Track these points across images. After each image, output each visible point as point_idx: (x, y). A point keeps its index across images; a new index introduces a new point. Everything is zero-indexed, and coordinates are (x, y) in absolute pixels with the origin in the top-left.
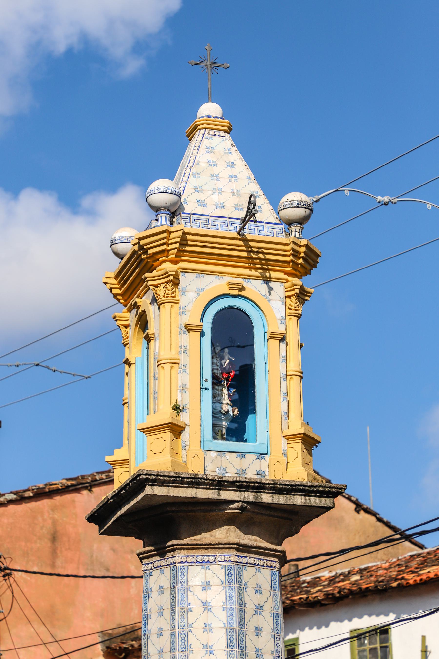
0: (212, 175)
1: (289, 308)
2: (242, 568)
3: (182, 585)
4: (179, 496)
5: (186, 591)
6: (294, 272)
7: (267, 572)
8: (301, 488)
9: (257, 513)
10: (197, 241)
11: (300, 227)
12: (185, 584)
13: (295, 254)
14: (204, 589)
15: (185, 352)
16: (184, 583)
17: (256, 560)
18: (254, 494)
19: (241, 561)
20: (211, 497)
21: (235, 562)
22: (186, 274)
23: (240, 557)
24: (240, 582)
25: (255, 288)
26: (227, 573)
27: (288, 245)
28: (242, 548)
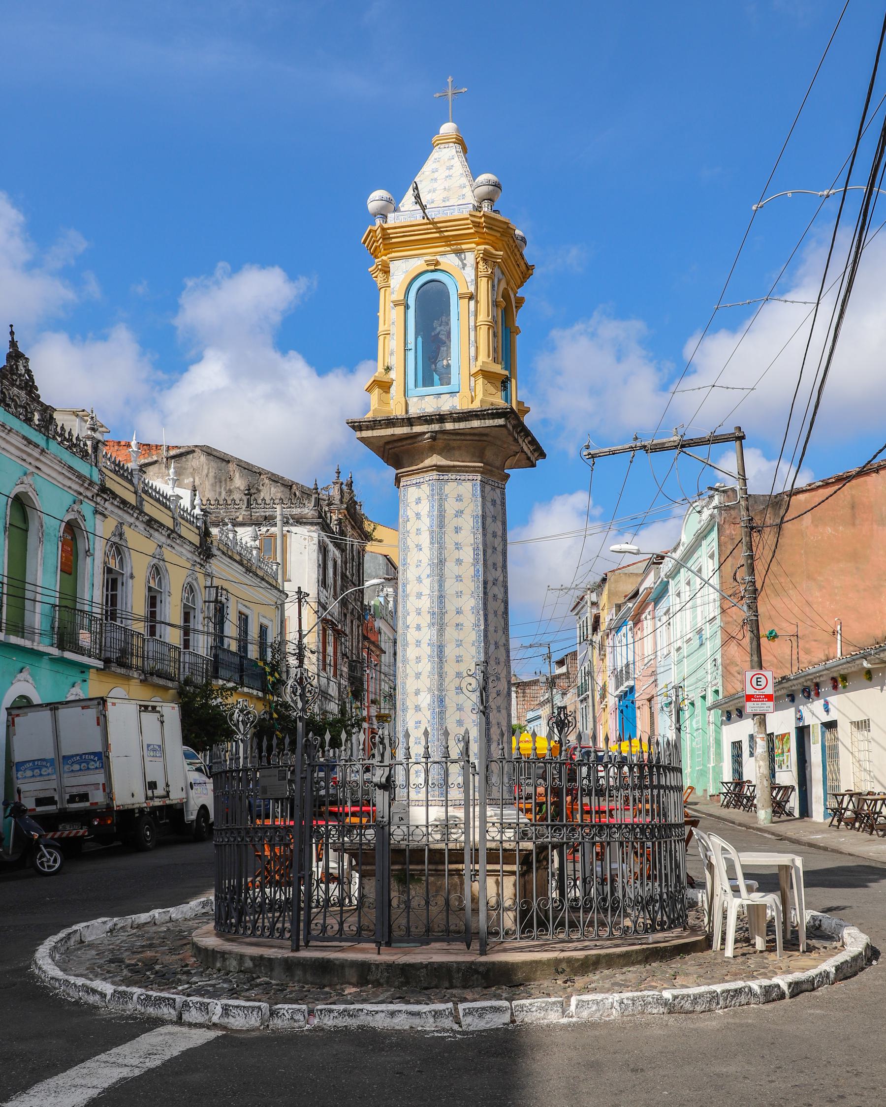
7: (469, 485)
13: (477, 225)
14: (417, 503)
15: (393, 323)
24: (439, 494)
25: (449, 261)
27: (467, 219)
28: (439, 469)
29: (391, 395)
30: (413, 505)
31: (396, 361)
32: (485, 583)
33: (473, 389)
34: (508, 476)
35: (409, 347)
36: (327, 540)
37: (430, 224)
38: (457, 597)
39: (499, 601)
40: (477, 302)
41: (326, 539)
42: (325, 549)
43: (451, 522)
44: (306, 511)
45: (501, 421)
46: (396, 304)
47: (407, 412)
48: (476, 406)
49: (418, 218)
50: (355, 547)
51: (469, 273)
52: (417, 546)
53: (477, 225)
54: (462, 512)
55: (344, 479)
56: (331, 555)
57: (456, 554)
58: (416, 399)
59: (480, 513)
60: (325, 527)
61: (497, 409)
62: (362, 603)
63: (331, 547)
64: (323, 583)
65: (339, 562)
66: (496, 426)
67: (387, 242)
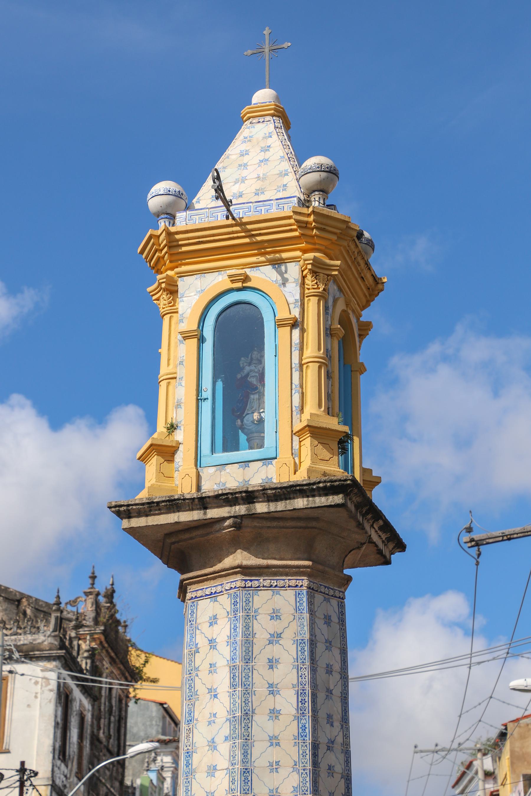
0: (240, 165)
1: (307, 288)
2: (251, 594)
3: (191, 624)
4: (159, 524)
5: (194, 630)
6: (310, 246)
7: (290, 594)
8: (298, 488)
9: (262, 528)
10: (188, 239)
11: (319, 194)
12: (194, 623)
14: (211, 624)
16: (193, 621)
17: (272, 581)
18: (246, 506)
19: (250, 585)
20: (195, 519)
21: (242, 587)
22: (185, 278)
23: (248, 581)
24: (247, 610)
25: (264, 276)
26: (233, 602)
28: (246, 571)
29: (175, 465)
30: (205, 627)
31: (184, 416)
32: (315, 747)
33: (295, 454)
34: (349, 579)
35: (204, 395)
36: (72, 683)
37: (236, 225)
38: (272, 771)
39: (338, 776)
40: (303, 331)
41: (69, 681)
42: (67, 697)
43: (262, 652)
44: (40, 638)
45: (338, 499)
46: (186, 336)
47: (199, 488)
48: (301, 477)
49: (220, 217)
50: (114, 692)
51: (292, 291)
52: (210, 690)
53: (303, 225)
54: (279, 636)
55: (101, 586)
56: (76, 706)
57: (270, 702)
58: (212, 470)
59: (307, 636)
60: (69, 662)
61: (331, 481)
62: (122, 782)
63: (77, 694)
64: (61, 753)
65: (89, 717)
66: (330, 506)
67: (175, 251)
